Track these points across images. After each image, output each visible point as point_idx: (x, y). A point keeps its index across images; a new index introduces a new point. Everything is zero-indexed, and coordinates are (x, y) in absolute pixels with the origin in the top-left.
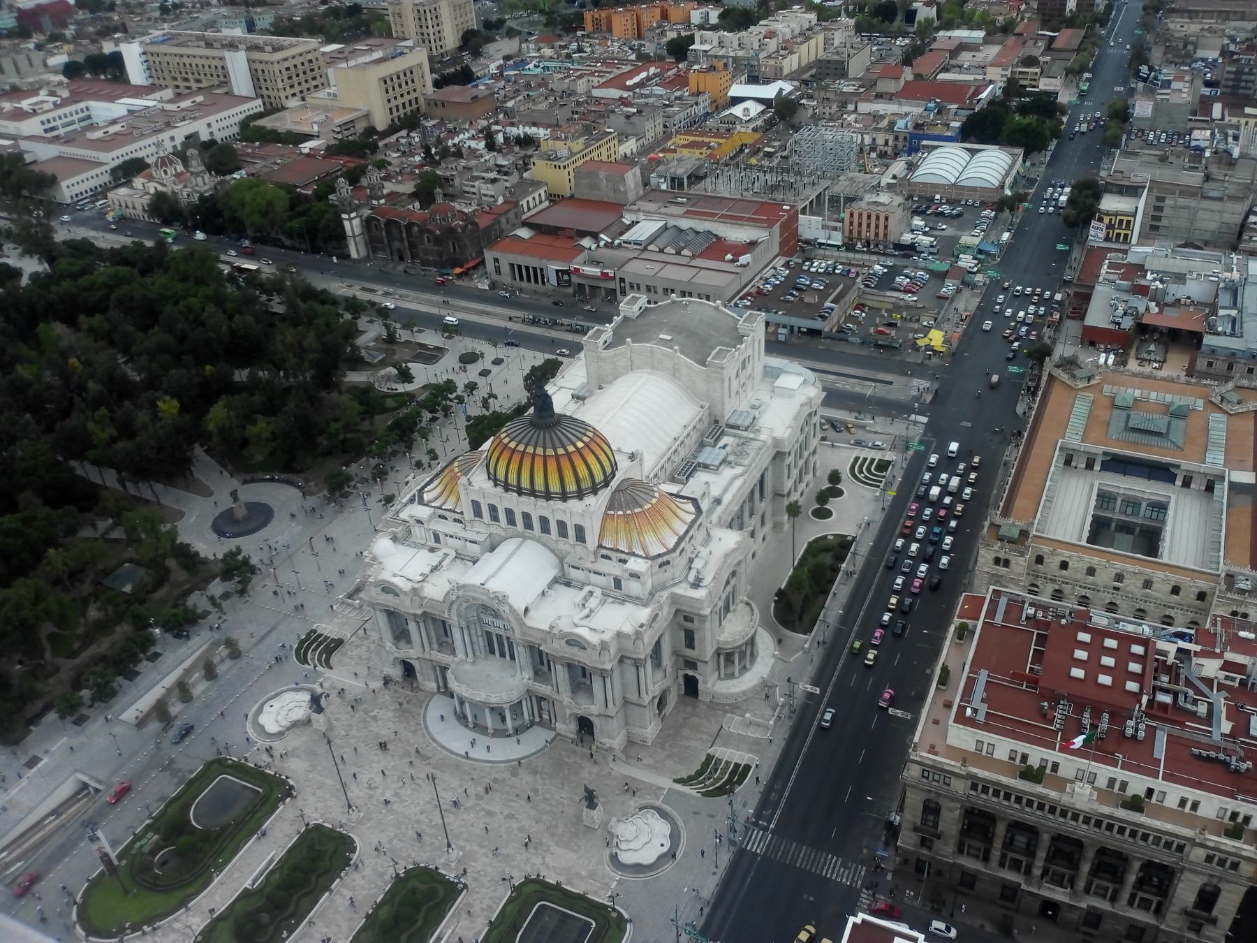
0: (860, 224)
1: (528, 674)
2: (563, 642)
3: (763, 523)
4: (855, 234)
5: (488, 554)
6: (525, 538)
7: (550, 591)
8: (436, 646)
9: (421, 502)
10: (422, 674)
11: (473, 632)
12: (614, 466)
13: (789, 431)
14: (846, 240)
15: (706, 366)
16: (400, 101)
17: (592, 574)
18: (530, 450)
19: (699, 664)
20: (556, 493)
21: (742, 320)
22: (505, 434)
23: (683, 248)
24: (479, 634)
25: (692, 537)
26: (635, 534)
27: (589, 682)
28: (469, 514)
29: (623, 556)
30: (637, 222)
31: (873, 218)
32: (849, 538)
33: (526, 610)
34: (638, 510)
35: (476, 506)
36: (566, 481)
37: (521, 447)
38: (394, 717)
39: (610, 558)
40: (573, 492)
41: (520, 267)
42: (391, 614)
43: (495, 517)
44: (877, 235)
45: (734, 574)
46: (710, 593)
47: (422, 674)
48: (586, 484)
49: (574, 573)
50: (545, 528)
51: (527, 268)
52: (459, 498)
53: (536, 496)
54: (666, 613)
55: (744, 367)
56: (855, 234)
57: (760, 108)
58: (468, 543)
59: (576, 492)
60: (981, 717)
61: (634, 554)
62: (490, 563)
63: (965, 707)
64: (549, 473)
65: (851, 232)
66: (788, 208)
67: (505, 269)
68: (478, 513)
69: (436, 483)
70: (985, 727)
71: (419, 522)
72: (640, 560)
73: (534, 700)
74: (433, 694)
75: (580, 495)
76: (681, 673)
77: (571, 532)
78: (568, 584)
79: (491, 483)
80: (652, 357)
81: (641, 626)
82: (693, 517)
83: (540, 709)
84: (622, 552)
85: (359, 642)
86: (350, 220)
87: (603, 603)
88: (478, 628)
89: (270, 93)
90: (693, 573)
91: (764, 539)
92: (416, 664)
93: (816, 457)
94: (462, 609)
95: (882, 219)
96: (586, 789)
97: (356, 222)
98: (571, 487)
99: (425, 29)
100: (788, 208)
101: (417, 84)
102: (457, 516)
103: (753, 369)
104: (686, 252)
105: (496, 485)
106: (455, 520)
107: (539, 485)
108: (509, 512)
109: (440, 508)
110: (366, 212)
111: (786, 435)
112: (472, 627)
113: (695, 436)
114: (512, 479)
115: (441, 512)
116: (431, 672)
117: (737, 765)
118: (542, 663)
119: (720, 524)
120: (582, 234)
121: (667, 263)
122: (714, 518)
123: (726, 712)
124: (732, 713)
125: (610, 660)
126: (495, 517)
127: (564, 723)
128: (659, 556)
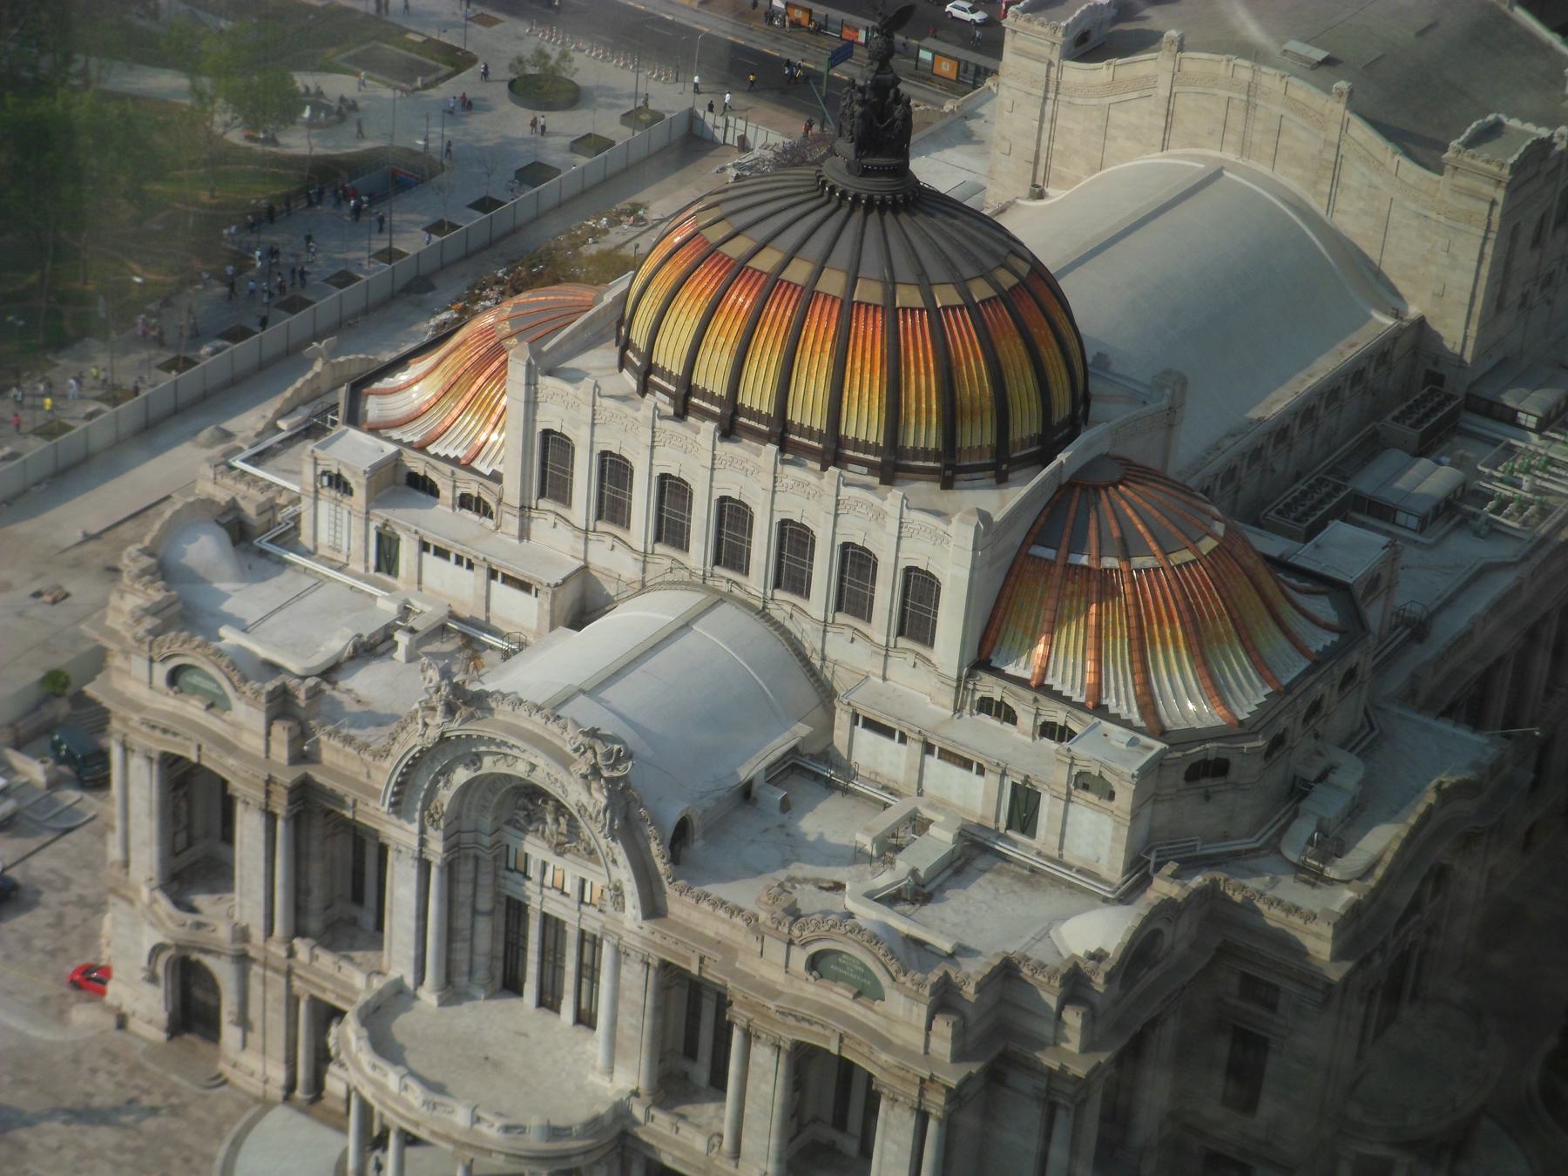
2: (800, 958)
5: (562, 630)
8: (314, 924)
9: (354, 418)
10: (244, 1022)
11: (464, 891)
12: (1082, 400)
15: (1439, 169)
18: (798, 272)
20: (866, 447)
24: (484, 903)
26: (1119, 649)
27: (851, 1146)
29: (1059, 715)
33: (682, 831)
37: (766, 261)
39: (1010, 716)
40: (926, 454)
43: (612, 508)
46: (1355, 910)
47: (244, 1022)
48: (977, 436)
53: (784, 445)
54: (1177, 937)
58: (497, 585)
59: (937, 456)
61: (1100, 710)
64: (855, 363)
71: (338, 483)
72: (1119, 735)
74: (266, 1104)
77: (885, 594)
79: (629, 381)
80: (1249, 106)
81: (1098, 956)
82: (1329, 639)
84: (1067, 701)
88: (485, 880)
98: (922, 432)
105: (645, 387)
106: (465, 502)
107: (808, 409)
108: (672, 491)
109: (421, 448)
112: (466, 871)
115: (416, 463)
116: (277, 1020)
118: (691, 1052)
119: (1410, 696)
122: (1397, 680)
125: (959, 1056)
126: (612, 508)
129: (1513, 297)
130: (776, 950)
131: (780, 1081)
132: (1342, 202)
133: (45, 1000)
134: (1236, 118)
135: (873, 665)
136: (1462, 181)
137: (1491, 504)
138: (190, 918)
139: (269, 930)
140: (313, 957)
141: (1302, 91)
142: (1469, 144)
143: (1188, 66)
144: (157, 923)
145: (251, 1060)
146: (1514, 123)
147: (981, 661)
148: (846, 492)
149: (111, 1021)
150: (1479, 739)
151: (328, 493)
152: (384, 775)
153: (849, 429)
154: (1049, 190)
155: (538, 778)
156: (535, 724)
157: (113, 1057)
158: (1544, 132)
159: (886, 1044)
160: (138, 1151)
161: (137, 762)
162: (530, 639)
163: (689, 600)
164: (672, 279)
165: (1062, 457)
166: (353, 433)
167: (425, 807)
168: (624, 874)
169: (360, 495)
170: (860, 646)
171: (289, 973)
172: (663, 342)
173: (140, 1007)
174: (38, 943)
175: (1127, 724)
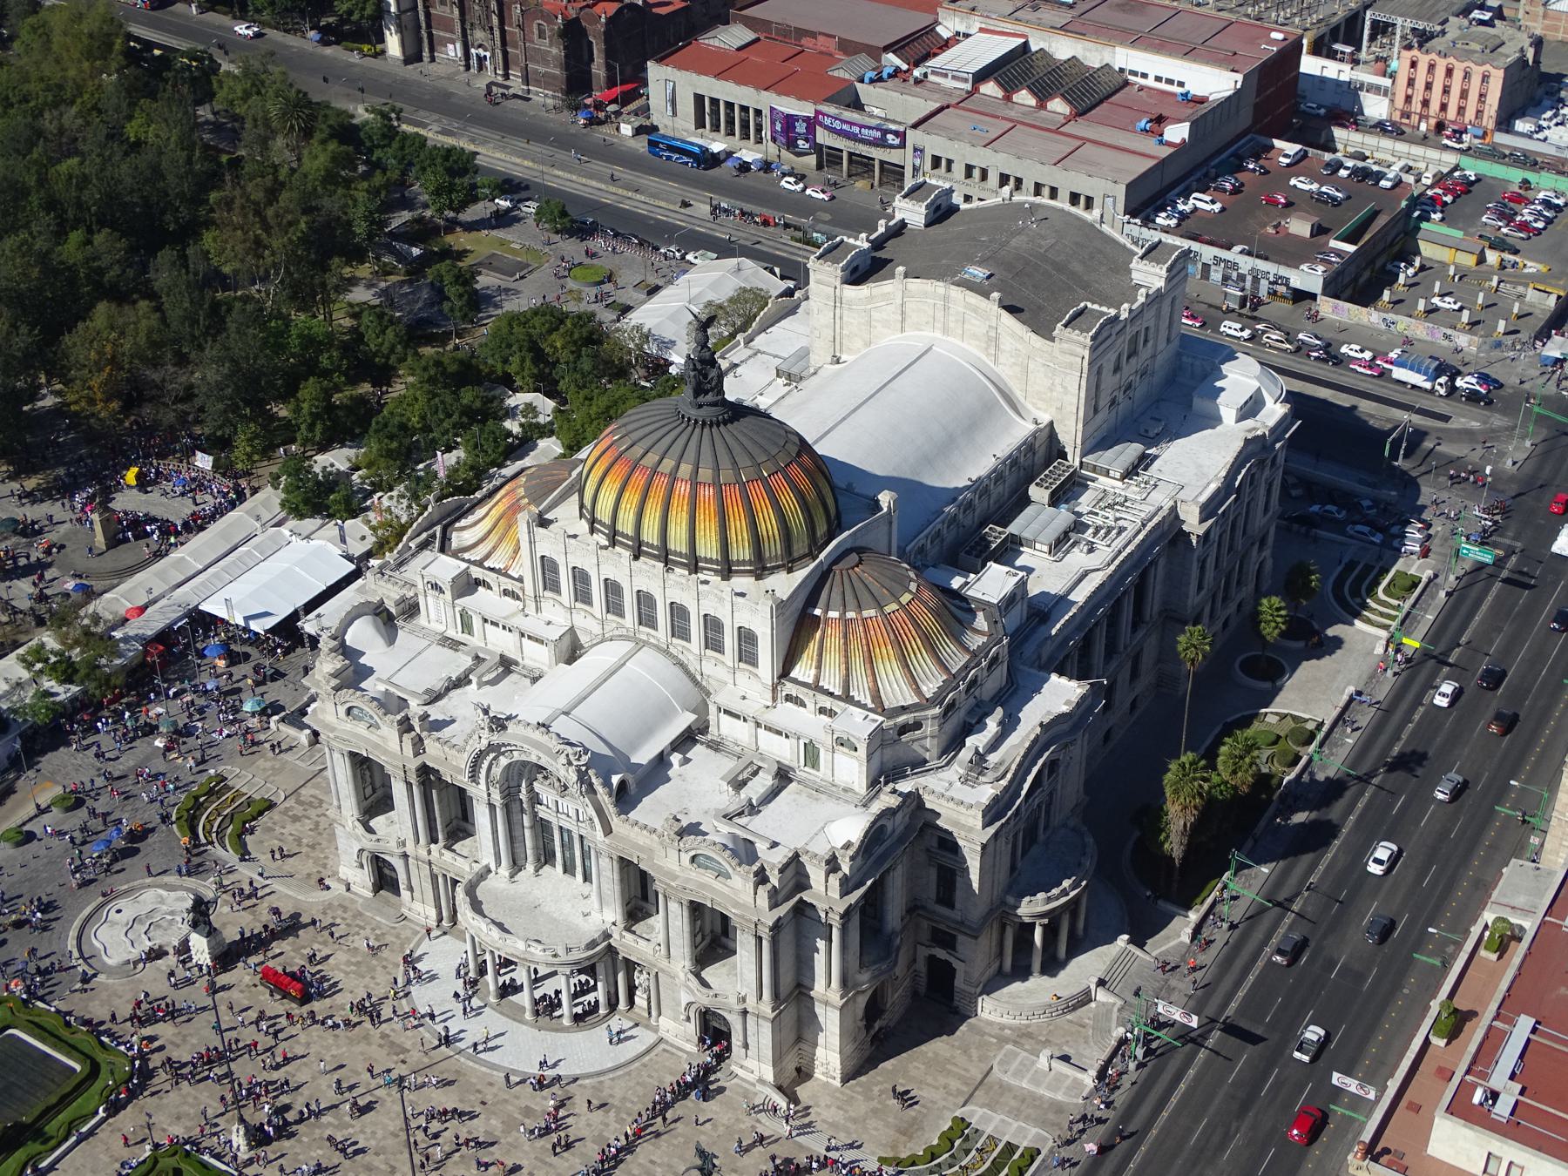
0: (1429, 86)
1: (612, 914)
2: (686, 858)
3: (1135, 674)
4: (1416, 106)
5: (562, 665)
6: (641, 644)
7: (675, 758)
10: (411, 889)
11: (516, 817)
13: (1213, 487)
14: (1396, 117)
15: (1052, 339)
17: (761, 731)
18: (668, 464)
19: (961, 938)
20: (710, 561)
21: (1141, 252)
22: (623, 431)
23: (1050, 97)
25: (974, 682)
30: (967, 36)
31: (1458, 75)
32: (1311, 726)
34: (872, 612)
35: (548, 568)
36: (732, 535)
38: (349, 963)
39: (803, 705)
40: (744, 563)
41: (714, 102)
42: (363, 766)
43: (583, 596)
44: (1461, 110)
45: (1052, 765)
47: (411, 889)
48: (773, 548)
49: (726, 728)
50: (680, 629)
51: (730, 106)
52: (517, 550)
55: (1133, 353)
56: (1416, 106)
59: (750, 563)
60: (1503, 1108)
62: (565, 682)
63: (1474, 1087)
64: (700, 517)
65: (1408, 99)
66: (1280, 36)
67: (687, 107)
68: (550, 581)
69: (480, 512)
70: (1512, 1129)
71: (435, 586)
73: (620, 965)
75: (760, 569)
76: (923, 952)
77: (730, 641)
78: (716, 746)
79: (584, 526)
80: (946, 308)
81: (847, 846)
83: (631, 990)
84: (831, 694)
85: (299, 810)
87: (773, 794)
90: (966, 754)
91: (1133, 706)
92: (398, 864)
93: (1267, 553)
94: (497, 771)
96: (701, 1153)
98: (742, 551)
100: (1280, 36)
102: (508, 584)
103: (1154, 356)
104: (1058, 106)
105: (592, 530)
106: (506, 593)
107: (678, 540)
108: (612, 588)
109: (480, 564)
111: (1203, 498)
112: (515, 807)
113: (1010, 480)
114: (626, 524)
115: (476, 572)
117: (1010, 1148)
118: (645, 897)
120: (850, 48)
121: (1016, 123)
123: (1003, 1040)
124: (1016, 1043)
126: (583, 596)
127: (675, 1019)
128: (904, 709)
129: (1104, 401)
130: (673, 854)
131: (686, 920)
132: (1002, 359)
133: (309, 875)
134: (940, 314)
135: (729, 678)
136: (1065, 346)
137: (1091, 530)
138: (374, 837)
139: (418, 841)
140: (441, 854)
141: (974, 299)
142: (1066, 326)
143: (910, 286)
144: (358, 839)
145: (417, 906)
146: (1096, 307)
147: (785, 674)
148: (702, 587)
149: (344, 888)
150: (1074, 684)
151: (430, 592)
152: (463, 761)
153: (701, 552)
154: (844, 358)
155: (542, 763)
156: (538, 735)
157: (345, 909)
158: (1113, 312)
159: (737, 904)
160: (358, 964)
161: (336, 755)
162: (545, 668)
163: (626, 647)
164: (603, 468)
165: (822, 556)
166: (443, 557)
167: (488, 776)
168: (591, 812)
169: (448, 595)
170: (720, 668)
171: (430, 863)
172: (599, 506)
173: (357, 880)
174: (305, 841)
175: (864, 707)
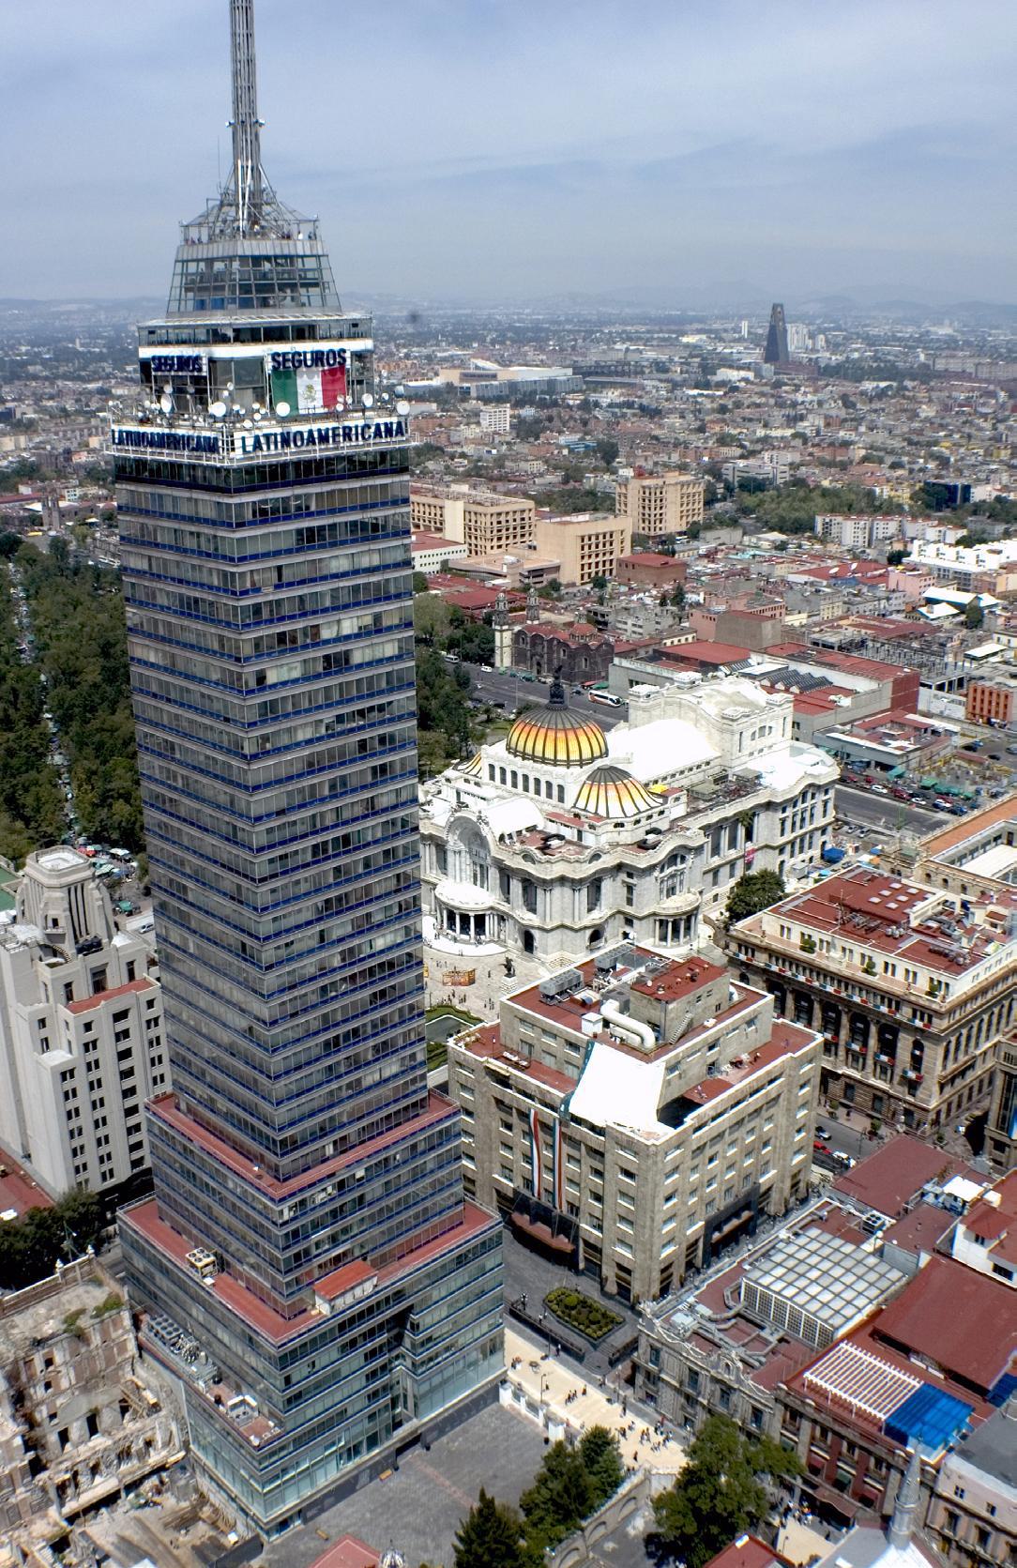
4: (978, 711)
16: (593, 560)
28: (485, 774)
35: (492, 767)
50: (538, 792)
56: (978, 711)
57: (956, 611)
65: (974, 707)
68: (492, 777)
75: (568, 763)
77: (555, 792)
86: (501, 631)
89: (479, 542)
95: (1002, 698)
97: (508, 635)
99: (647, 511)
101: (616, 546)
110: (517, 628)
